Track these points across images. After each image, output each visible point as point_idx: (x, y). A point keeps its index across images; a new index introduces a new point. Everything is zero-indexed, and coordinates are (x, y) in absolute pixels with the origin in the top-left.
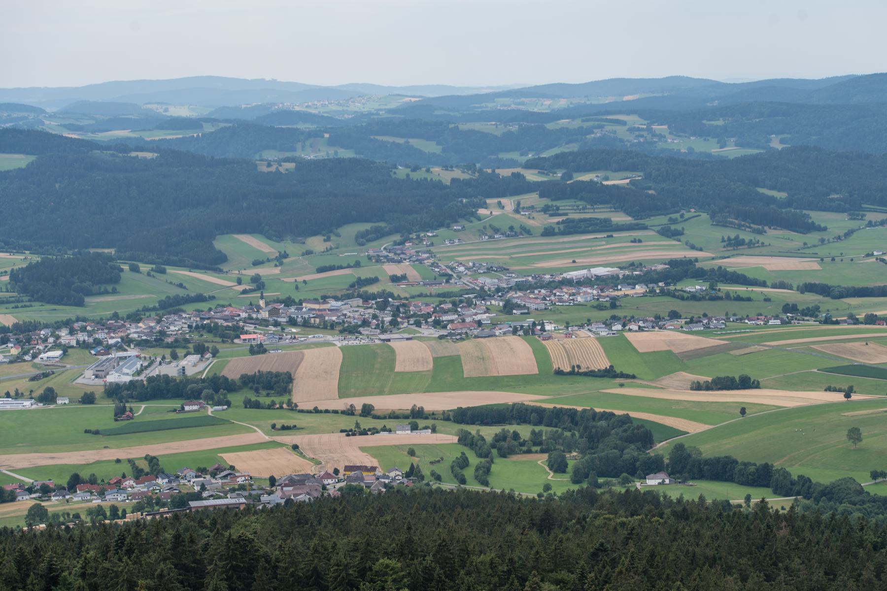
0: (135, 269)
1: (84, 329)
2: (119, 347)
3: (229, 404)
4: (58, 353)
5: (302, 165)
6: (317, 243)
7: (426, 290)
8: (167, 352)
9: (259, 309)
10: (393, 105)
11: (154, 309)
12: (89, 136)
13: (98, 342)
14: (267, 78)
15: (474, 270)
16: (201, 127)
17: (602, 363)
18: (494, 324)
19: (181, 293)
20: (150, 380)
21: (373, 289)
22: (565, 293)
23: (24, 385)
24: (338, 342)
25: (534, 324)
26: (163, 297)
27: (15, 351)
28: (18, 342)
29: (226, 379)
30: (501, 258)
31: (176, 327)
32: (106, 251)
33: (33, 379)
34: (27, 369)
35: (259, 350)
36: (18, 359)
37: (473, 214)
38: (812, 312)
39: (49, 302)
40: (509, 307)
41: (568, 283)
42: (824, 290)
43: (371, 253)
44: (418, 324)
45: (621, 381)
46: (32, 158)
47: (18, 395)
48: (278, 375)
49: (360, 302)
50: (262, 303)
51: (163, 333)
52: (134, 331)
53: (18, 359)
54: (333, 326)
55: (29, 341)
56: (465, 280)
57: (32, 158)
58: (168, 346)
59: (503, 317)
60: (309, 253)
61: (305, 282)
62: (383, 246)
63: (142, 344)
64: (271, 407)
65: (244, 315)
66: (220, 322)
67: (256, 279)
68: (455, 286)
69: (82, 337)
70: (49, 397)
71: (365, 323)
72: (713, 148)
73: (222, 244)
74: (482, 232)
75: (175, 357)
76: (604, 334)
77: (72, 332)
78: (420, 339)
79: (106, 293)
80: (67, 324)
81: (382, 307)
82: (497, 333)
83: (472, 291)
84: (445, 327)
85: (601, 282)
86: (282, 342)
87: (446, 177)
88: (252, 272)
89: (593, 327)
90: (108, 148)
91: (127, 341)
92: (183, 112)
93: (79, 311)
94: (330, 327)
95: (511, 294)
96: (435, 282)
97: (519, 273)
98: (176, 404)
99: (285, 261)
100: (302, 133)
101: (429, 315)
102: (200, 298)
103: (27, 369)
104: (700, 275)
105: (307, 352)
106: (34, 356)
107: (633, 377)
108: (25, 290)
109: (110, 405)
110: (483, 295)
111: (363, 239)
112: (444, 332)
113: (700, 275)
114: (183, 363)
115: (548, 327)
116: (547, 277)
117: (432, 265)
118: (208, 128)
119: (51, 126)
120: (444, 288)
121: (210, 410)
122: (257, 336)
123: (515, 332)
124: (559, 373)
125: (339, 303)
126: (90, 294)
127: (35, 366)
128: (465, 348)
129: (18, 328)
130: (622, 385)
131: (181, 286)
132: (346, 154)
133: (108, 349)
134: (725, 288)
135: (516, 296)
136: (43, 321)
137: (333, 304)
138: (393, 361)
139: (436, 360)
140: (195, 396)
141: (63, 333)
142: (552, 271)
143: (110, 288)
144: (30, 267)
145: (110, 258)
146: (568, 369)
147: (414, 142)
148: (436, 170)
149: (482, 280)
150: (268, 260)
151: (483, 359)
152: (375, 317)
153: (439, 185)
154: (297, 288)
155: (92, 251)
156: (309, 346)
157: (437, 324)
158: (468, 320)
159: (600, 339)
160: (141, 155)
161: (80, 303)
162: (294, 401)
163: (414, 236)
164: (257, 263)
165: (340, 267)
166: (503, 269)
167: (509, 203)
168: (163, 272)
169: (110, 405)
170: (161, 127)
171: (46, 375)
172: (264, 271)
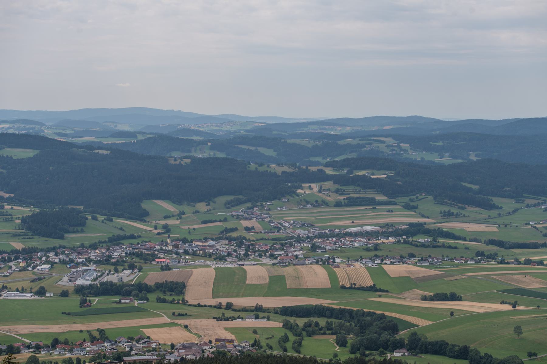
0: (95, 218)
1: (63, 253)
2: (84, 264)
3: (147, 299)
4: (48, 266)
6: (202, 207)
7: (266, 236)
9: (167, 244)
10: (249, 128)
11: (105, 242)
12: (70, 140)
13: (72, 261)
14: (176, 109)
15: (294, 226)
16: (136, 137)
17: (369, 283)
18: (305, 258)
19: (122, 233)
20: (102, 284)
21: (234, 235)
23: (27, 284)
25: (329, 258)
26: (111, 235)
27: (22, 265)
28: (25, 259)
29: (147, 285)
30: (310, 219)
31: (118, 253)
32: (78, 207)
33: (33, 281)
35: (166, 268)
36: (24, 269)
38: (493, 256)
39: (43, 236)
40: (314, 248)
41: (350, 234)
42: (500, 244)
43: (234, 213)
44: (260, 256)
45: (378, 293)
46: (37, 152)
47: (23, 291)
48: (177, 283)
49: (227, 242)
51: (110, 257)
52: (93, 255)
53: (24, 269)
54: (210, 255)
55: (31, 258)
56: (289, 231)
57: (37, 152)
58: (113, 264)
59: (311, 253)
60: (197, 212)
61: (194, 229)
62: (241, 209)
63: (97, 263)
64: (172, 302)
65: (158, 247)
66: (144, 251)
67: (165, 227)
68: (283, 234)
69: (62, 257)
70: (41, 292)
71: (229, 254)
72: (436, 159)
73: (146, 205)
74: (299, 203)
75: (116, 271)
76: (370, 265)
77: (56, 254)
78: (262, 265)
79: (77, 232)
80: (54, 249)
81: (240, 245)
82: (307, 263)
83: (293, 237)
84: (276, 258)
86: (180, 264)
87: (279, 170)
88: (163, 222)
91: (89, 260)
94: (208, 256)
96: (271, 231)
97: (321, 228)
98: (116, 298)
99: (183, 216)
100: (195, 142)
101: (267, 251)
102: (132, 237)
104: (427, 232)
106: (34, 268)
107: (387, 291)
108: (29, 229)
109: (77, 299)
110: (299, 240)
111: (229, 205)
112: (276, 261)
113: (427, 232)
114: (121, 274)
115: (337, 260)
116: (337, 230)
117: (270, 221)
118: (140, 137)
119: (48, 133)
120: (276, 235)
121: (136, 303)
122: (165, 260)
123: (317, 262)
124: (343, 287)
125: (214, 242)
126: (68, 232)
127: (34, 273)
128: (288, 271)
129: (25, 251)
130: (380, 296)
131: (121, 229)
132: (220, 155)
133: (78, 264)
134: (442, 240)
135: (319, 242)
136: (39, 247)
137: (211, 242)
138: (245, 277)
139: (270, 277)
140: (127, 294)
141: (51, 254)
142: (340, 227)
143: (79, 229)
144: (34, 215)
145: (80, 212)
146: (349, 286)
147: (262, 150)
148: (273, 166)
149: (298, 231)
150: (173, 216)
151: (298, 278)
152: (235, 251)
153: (275, 175)
154: (189, 232)
155: (70, 207)
156: (196, 267)
157: (272, 256)
158: (290, 254)
159: (368, 269)
160: (101, 152)
161: (62, 238)
162: (186, 299)
163: (259, 204)
164: (166, 217)
165: (215, 221)
166: (311, 225)
167: (315, 187)
168: (111, 220)
169: (77, 299)
171: (40, 279)
172: (170, 222)
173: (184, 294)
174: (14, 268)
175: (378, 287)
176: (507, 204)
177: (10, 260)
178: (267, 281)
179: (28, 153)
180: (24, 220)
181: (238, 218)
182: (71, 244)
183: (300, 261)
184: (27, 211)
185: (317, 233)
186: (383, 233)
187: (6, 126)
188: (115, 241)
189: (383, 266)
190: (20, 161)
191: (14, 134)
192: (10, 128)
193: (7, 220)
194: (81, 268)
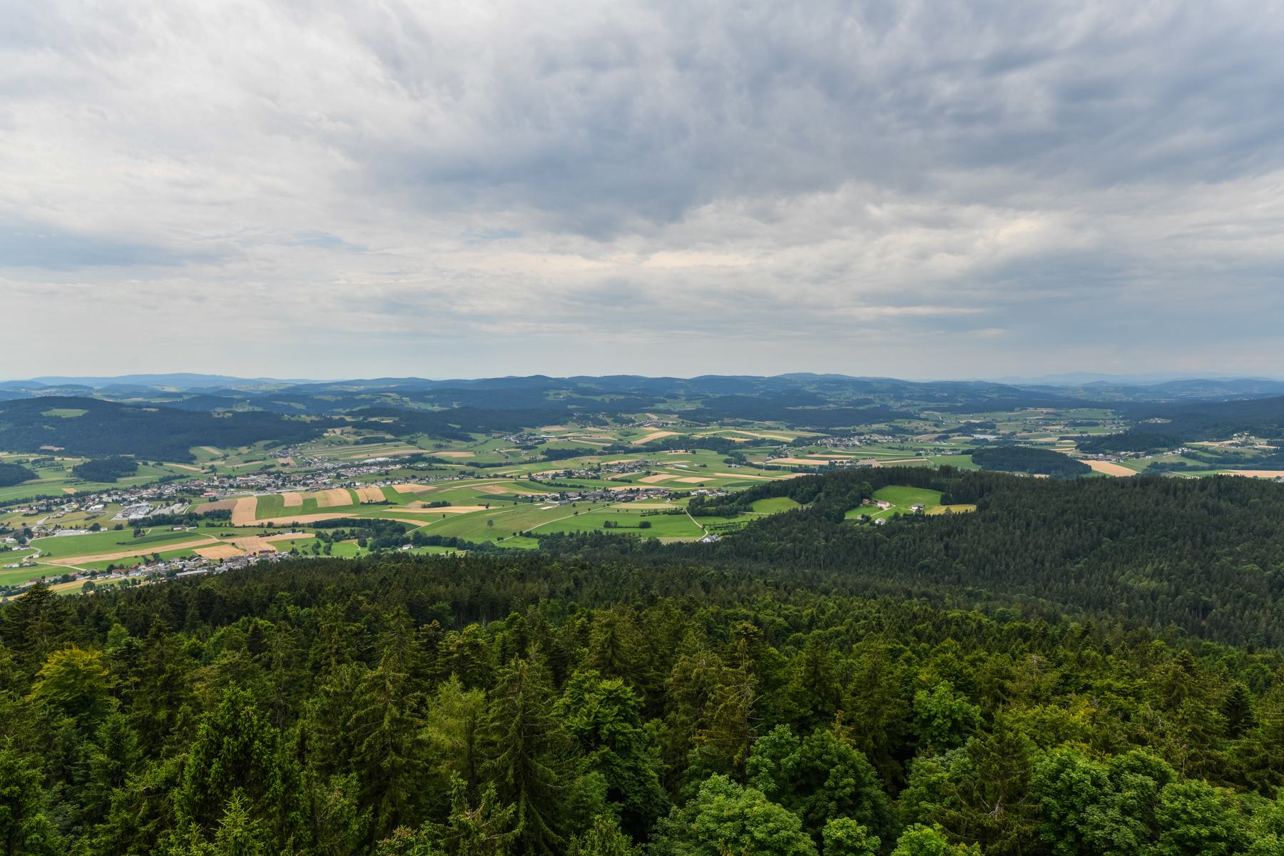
1: (116, 494)
2: (138, 502)
4: (102, 506)
5: (235, 414)
6: (244, 450)
7: (300, 469)
8: (164, 503)
9: (214, 480)
10: (282, 388)
11: (157, 482)
12: (119, 401)
13: (125, 500)
14: (217, 375)
15: (322, 461)
17: (383, 499)
19: (172, 474)
20: (154, 517)
21: (272, 470)
22: (365, 469)
23: (81, 523)
24: (255, 494)
26: (161, 477)
27: (75, 506)
29: (196, 514)
30: (335, 455)
31: (169, 491)
33: (86, 519)
34: (83, 514)
35: (215, 499)
36: (78, 510)
37: (322, 436)
38: (472, 474)
39: (96, 481)
40: (339, 476)
41: (366, 464)
42: (477, 465)
43: (271, 453)
44: (295, 485)
46: (86, 411)
47: (77, 528)
48: (224, 511)
49: (266, 476)
50: (215, 478)
51: (161, 494)
52: (145, 494)
53: (78, 510)
55: (84, 500)
56: (318, 465)
57: (86, 411)
58: (164, 500)
59: (336, 480)
60: (239, 454)
62: (277, 451)
63: (148, 500)
65: (205, 484)
67: (212, 467)
68: (313, 467)
69: (115, 497)
70: (96, 528)
71: (269, 485)
73: (193, 451)
74: (326, 443)
75: (168, 505)
77: (109, 495)
78: (296, 491)
79: (129, 476)
80: (107, 491)
81: (277, 478)
85: (381, 464)
87: (308, 419)
88: (210, 464)
89: (378, 483)
90: (130, 406)
91: (141, 498)
92: (172, 390)
93: (114, 485)
95: (340, 470)
96: (303, 465)
97: (343, 461)
98: (169, 527)
101: (301, 481)
102: (182, 477)
103: (83, 514)
104: (424, 460)
105: (239, 500)
106: (87, 508)
108: (81, 476)
109: (132, 530)
110: (326, 471)
111: (267, 448)
113: (424, 460)
114: (173, 508)
118: (186, 397)
120: (308, 468)
121: (188, 530)
122: (214, 494)
123: (342, 486)
124: (363, 503)
126: (120, 476)
127: (88, 513)
128: (318, 495)
129: (77, 495)
131: (171, 471)
132: (257, 409)
133: (131, 502)
135: (342, 471)
137: (252, 477)
140: (179, 523)
143: (131, 473)
144: (85, 464)
145: (131, 459)
147: (292, 404)
148: (303, 416)
149: (325, 464)
152: (274, 482)
153: (305, 423)
155: (121, 456)
156: (240, 497)
157: (304, 484)
160: (149, 409)
161: (114, 481)
164: (212, 460)
165: (256, 460)
167: (338, 431)
168: (162, 465)
169: (132, 530)
170: (160, 397)
171: (94, 517)
172: (215, 463)
173: (230, 519)
174: (67, 510)
175: (389, 501)
176: (480, 437)
177: (62, 503)
178: (301, 503)
179: (78, 413)
180: (75, 469)
181: (275, 457)
182: (124, 486)
183: (328, 486)
184: (78, 461)
185: (340, 465)
186: (392, 462)
187: (54, 390)
188: (166, 481)
189: (393, 486)
190: (70, 420)
191: (62, 398)
192: (57, 392)
193: (58, 470)
194: (134, 505)
